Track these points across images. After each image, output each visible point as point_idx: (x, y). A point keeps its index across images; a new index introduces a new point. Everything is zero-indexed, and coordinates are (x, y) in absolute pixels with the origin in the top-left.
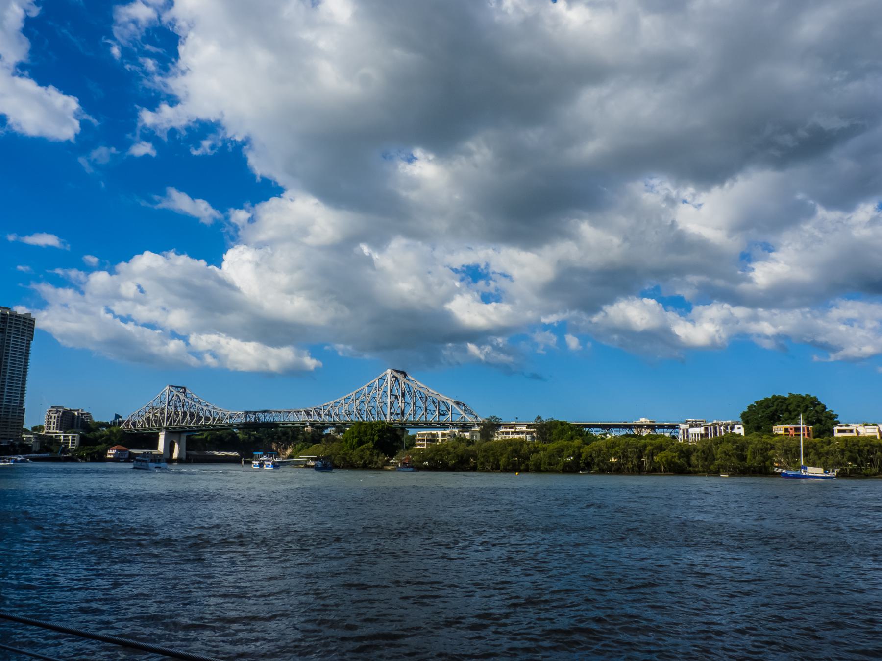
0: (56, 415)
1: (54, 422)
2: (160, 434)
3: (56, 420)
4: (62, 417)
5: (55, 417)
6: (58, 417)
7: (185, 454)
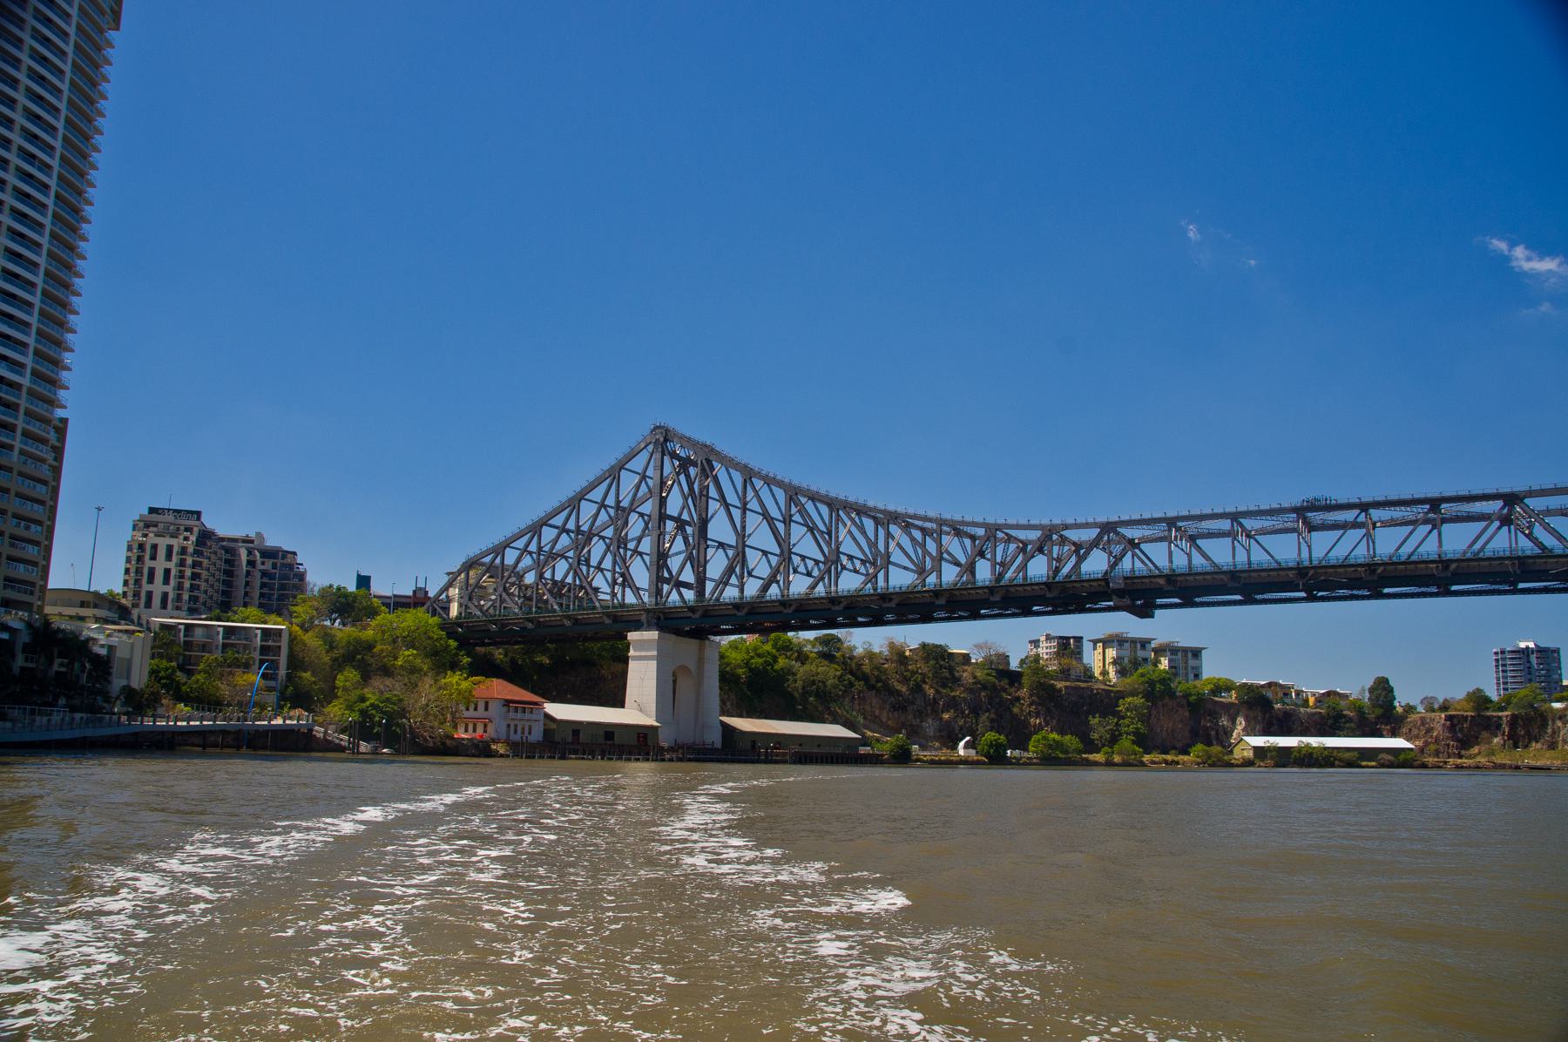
0: (173, 541)
1: (167, 572)
2: (632, 636)
3: (172, 565)
4: (197, 553)
5: (170, 549)
6: (183, 551)
7: (721, 728)
